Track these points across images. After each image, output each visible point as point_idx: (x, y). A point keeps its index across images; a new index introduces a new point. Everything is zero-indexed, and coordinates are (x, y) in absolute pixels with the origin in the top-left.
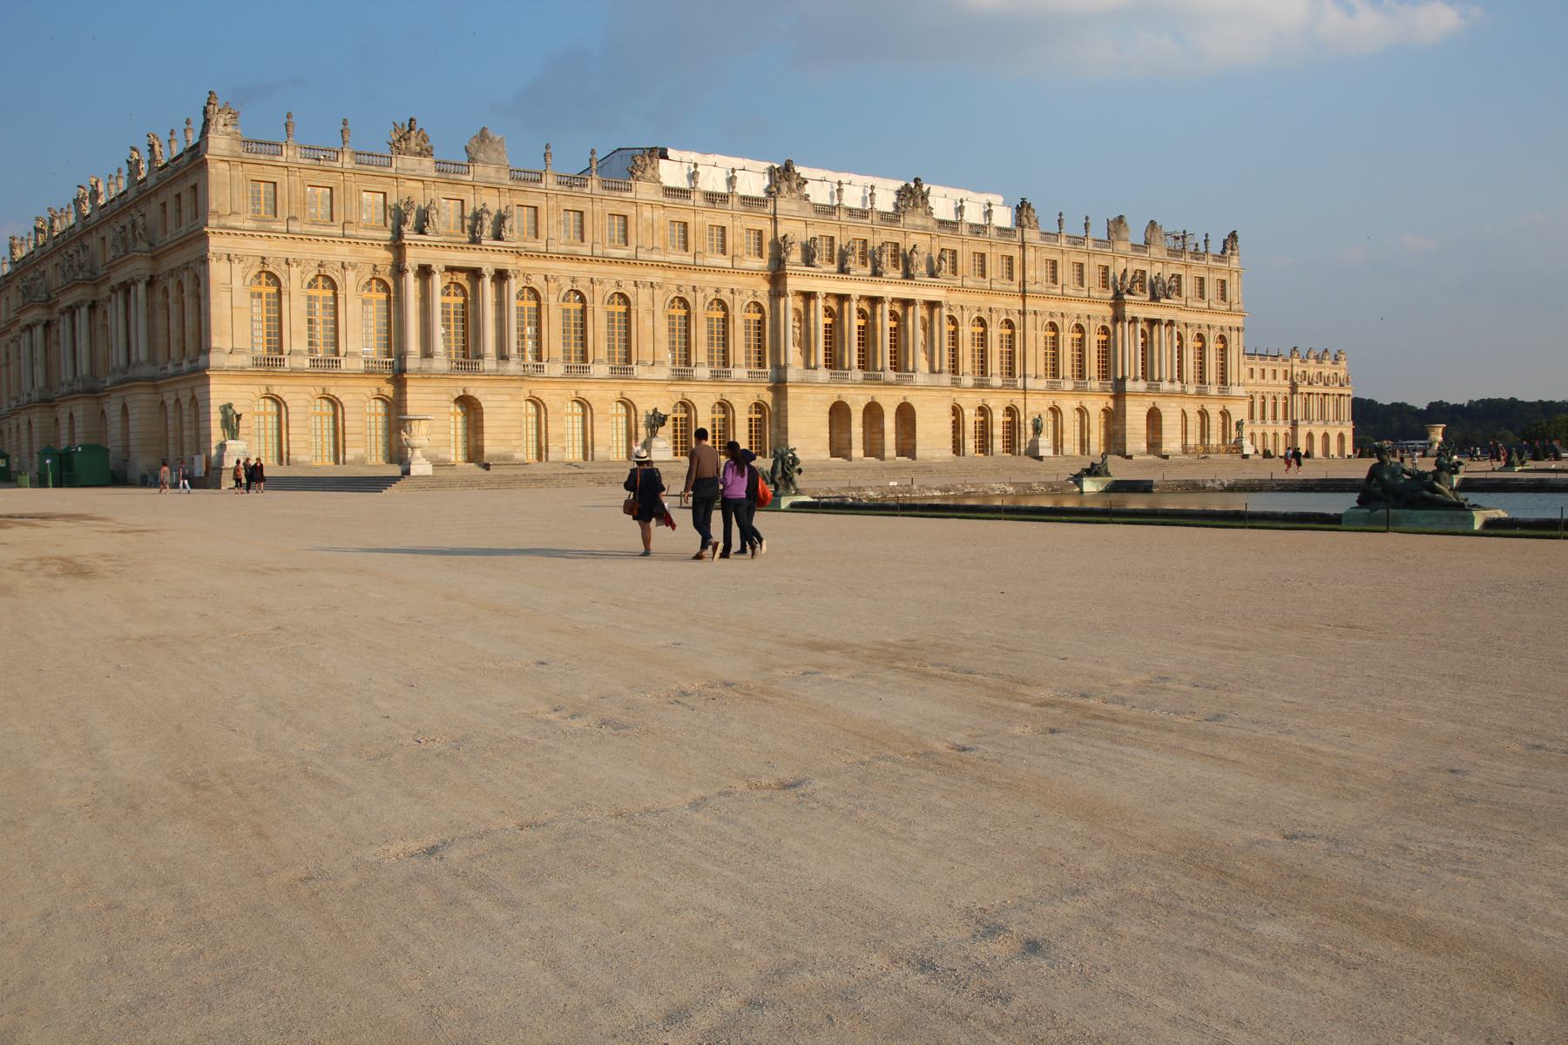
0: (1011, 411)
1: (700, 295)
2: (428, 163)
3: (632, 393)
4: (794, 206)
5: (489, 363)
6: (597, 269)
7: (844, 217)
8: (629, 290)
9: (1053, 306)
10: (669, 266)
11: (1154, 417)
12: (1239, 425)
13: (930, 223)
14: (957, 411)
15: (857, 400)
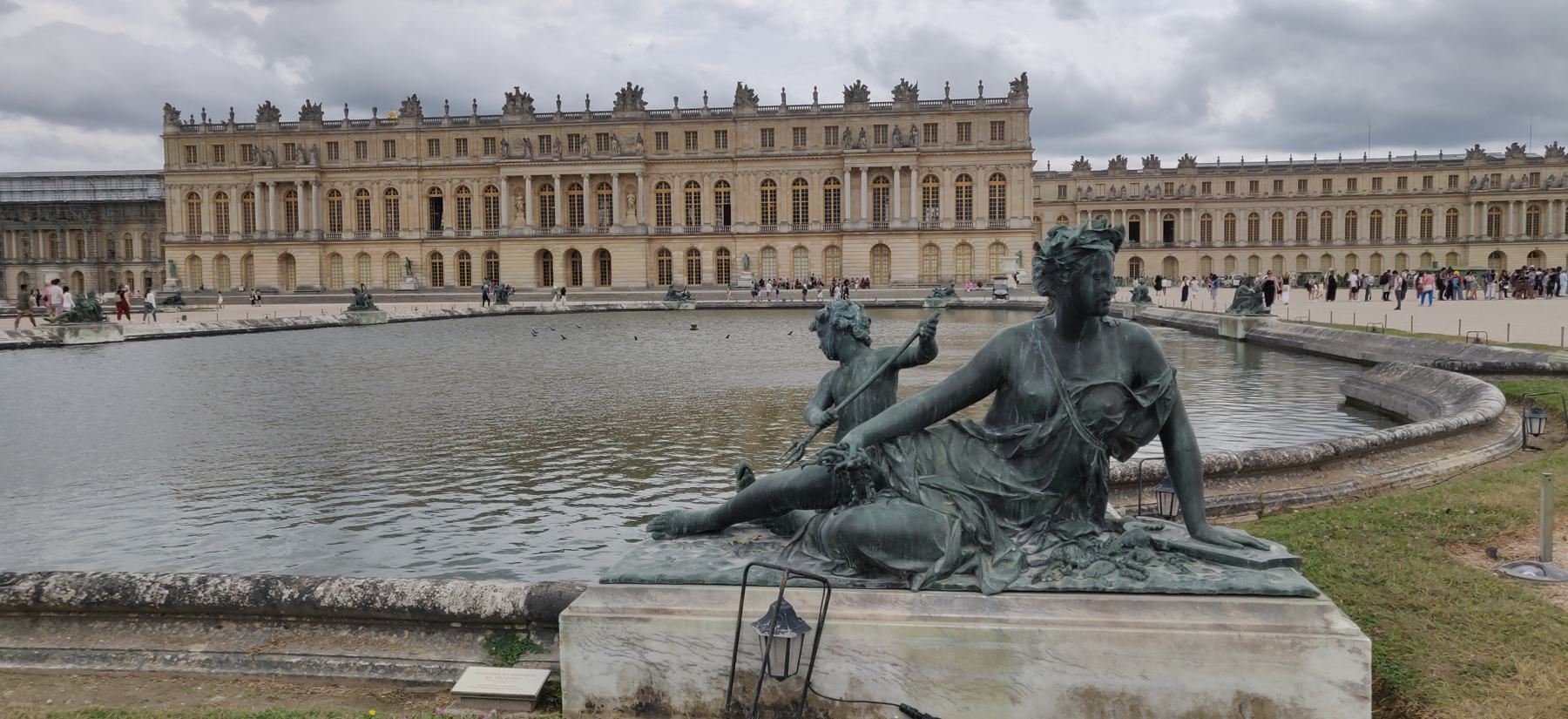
0: (722, 251)
1: (448, 185)
2: (274, 125)
3: (396, 248)
4: (518, 119)
5: (299, 235)
6: (375, 176)
7: (557, 119)
8: (396, 185)
9: (767, 166)
10: (421, 169)
11: (881, 250)
12: (1020, 254)
13: (639, 114)
14: (664, 252)
15: (559, 250)
